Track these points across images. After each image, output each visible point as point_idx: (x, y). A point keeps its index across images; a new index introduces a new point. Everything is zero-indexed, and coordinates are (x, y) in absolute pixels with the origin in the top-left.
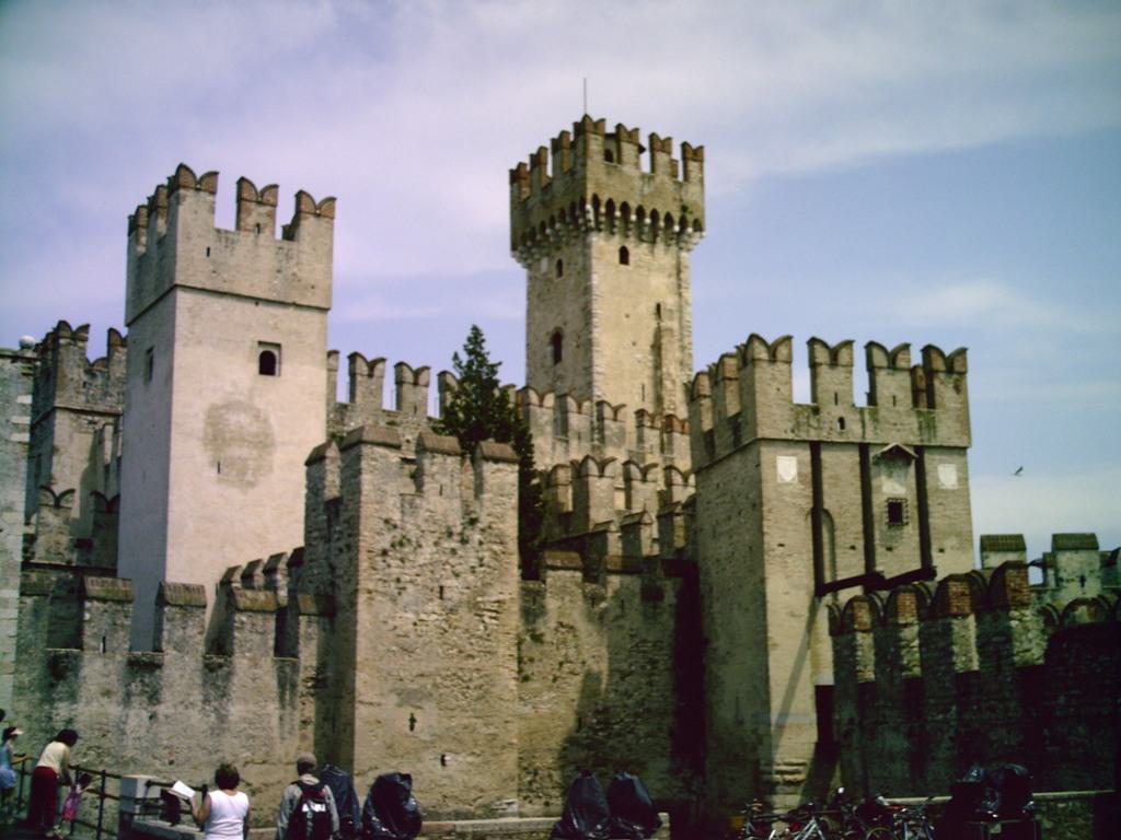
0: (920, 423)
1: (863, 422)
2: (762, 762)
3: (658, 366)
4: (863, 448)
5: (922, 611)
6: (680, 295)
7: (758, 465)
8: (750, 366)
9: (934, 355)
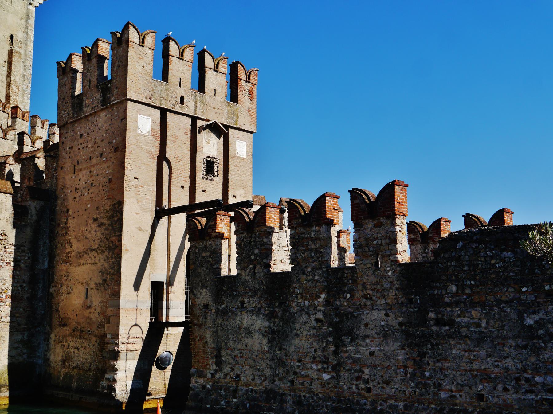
0: (229, 111)
1: (196, 102)
2: (109, 336)
3: (9, 75)
4: (194, 120)
5: (292, 222)
6: (27, 34)
7: (125, 118)
8: (124, 44)
9: (240, 67)
